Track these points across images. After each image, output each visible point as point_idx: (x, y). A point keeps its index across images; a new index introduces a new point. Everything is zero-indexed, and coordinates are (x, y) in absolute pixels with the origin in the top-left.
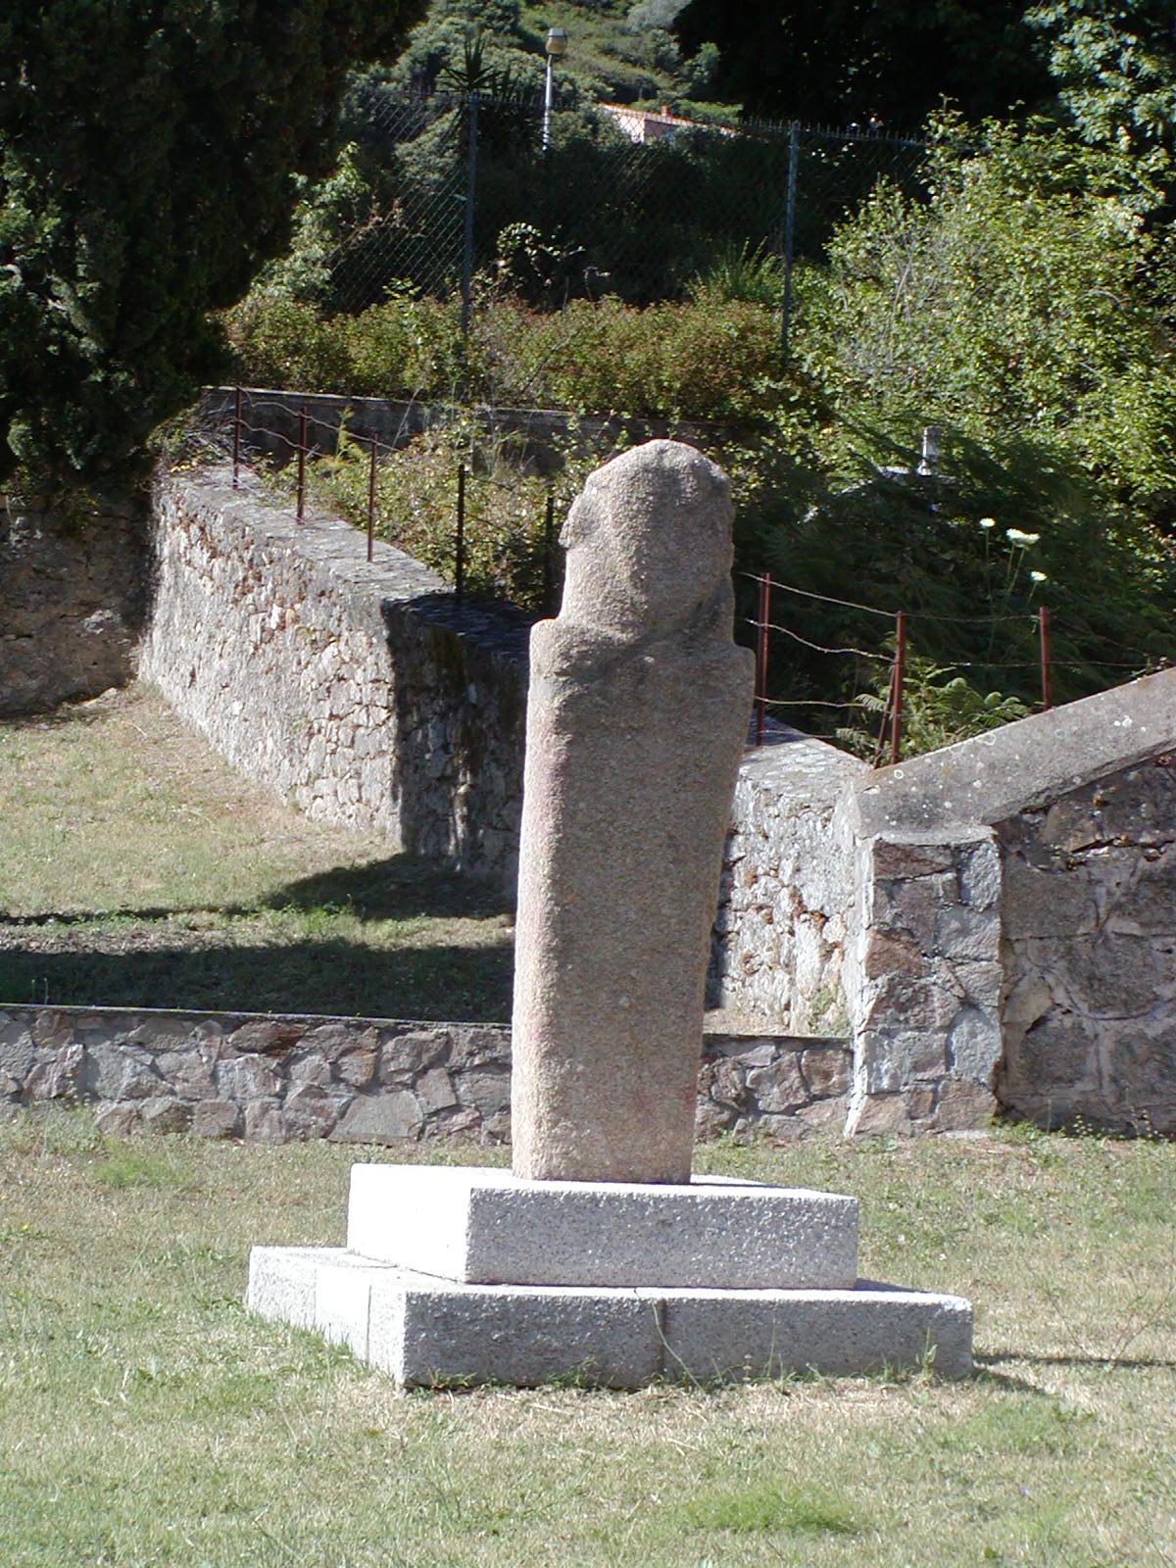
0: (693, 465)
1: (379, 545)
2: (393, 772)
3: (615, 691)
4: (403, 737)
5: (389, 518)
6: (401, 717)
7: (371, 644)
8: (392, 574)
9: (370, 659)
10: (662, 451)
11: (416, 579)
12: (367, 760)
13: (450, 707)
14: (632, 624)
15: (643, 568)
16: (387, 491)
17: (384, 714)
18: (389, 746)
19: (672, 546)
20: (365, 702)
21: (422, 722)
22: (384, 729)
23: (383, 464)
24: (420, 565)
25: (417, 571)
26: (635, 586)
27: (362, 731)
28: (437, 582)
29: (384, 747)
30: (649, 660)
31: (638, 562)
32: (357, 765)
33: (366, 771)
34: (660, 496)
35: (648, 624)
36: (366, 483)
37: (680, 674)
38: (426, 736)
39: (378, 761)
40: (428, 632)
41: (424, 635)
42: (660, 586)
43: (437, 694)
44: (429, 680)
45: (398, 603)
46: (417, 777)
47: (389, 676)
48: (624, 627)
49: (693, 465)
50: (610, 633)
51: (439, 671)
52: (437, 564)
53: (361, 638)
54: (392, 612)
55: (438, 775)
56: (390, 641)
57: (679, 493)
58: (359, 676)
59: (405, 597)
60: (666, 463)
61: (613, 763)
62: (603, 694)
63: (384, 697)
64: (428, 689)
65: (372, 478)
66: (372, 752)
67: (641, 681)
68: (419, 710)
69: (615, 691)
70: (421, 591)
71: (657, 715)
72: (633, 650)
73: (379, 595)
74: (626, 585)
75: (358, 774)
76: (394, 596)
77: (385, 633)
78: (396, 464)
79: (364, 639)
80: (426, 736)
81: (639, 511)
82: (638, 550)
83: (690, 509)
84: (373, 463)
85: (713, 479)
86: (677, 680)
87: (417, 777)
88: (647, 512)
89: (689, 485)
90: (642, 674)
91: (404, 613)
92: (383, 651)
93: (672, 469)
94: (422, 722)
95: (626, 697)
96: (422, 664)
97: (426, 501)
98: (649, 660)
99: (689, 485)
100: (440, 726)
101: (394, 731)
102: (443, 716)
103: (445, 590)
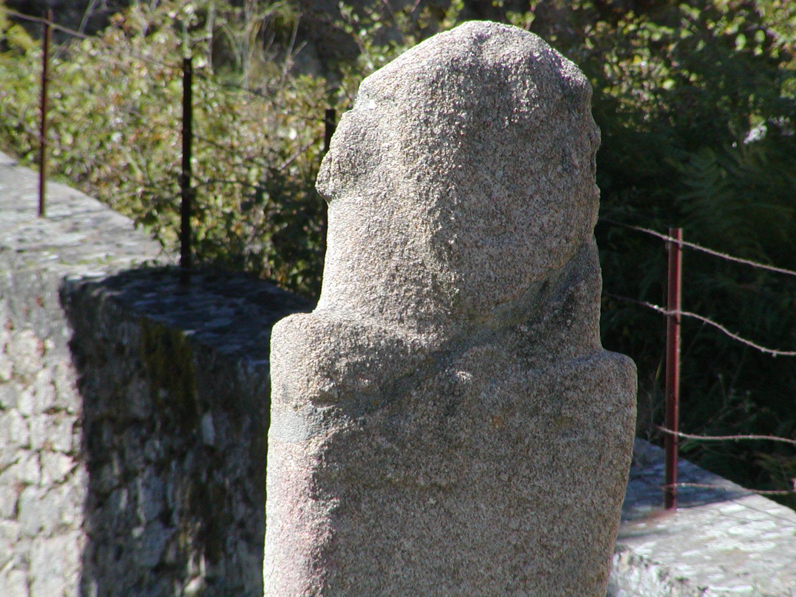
0: (531, 61)
1: (57, 190)
2: (83, 559)
3: (408, 428)
4: (97, 501)
5: (74, 146)
6: (94, 469)
7: (44, 351)
8: (75, 237)
9: (43, 376)
10: (481, 39)
11: (113, 243)
12: (40, 540)
13: (171, 452)
14: (436, 319)
15: (451, 228)
16: (70, 100)
17: (65, 464)
18: (74, 516)
19: (499, 191)
20: (36, 444)
21: (128, 476)
22: (66, 489)
23: (65, 57)
24: (122, 220)
25: (118, 231)
26: (439, 257)
27: (30, 492)
28: (148, 248)
29: (67, 519)
30: (464, 376)
31: (445, 217)
32: (23, 547)
33: (38, 558)
34: (479, 112)
35: (461, 318)
36: (36, 89)
37: (515, 398)
38: (133, 500)
39: (58, 542)
40: (136, 329)
41: (130, 334)
42: (480, 257)
43: (152, 429)
44: (138, 408)
45: (87, 284)
46: (120, 567)
47: (73, 402)
48: (422, 323)
49: (531, 61)
50: (400, 333)
51: (153, 394)
52: (149, 219)
53: (27, 341)
54: (76, 299)
55: (154, 562)
56: (74, 346)
57: (509, 106)
58: (26, 403)
59: (98, 273)
60: (488, 57)
61: (408, 545)
62: (391, 433)
63: (65, 437)
64: (136, 422)
65: (45, 80)
66: (49, 526)
67: (451, 410)
68: (122, 455)
69: (408, 428)
70: (124, 263)
71: (478, 466)
72: (439, 359)
73: (56, 270)
74: (426, 255)
75: (25, 562)
76: (79, 272)
77: (67, 333)
78: (85, 57)
79: (34, 343)
80: (133, 500)
81: (444, 135)
82: (443, 198)
83: (526, 133)
84: (45, 59)
85: (563, 83)
86: (509, 408)
87: (120, 567)
88: (457, 136)
89: (524, 93)
90: (452, 399)
91: (97, 300)
92: (63, 361)
93: (498, 67)
94: (128, 476)
95: (426, 438)
96: (126, 382)
97: (135, 116)
98: (464, 376)
99: (524, 93)
100: (156, 482)
101: (83, 492)
102: (161, 467)
103: (164, 260)
